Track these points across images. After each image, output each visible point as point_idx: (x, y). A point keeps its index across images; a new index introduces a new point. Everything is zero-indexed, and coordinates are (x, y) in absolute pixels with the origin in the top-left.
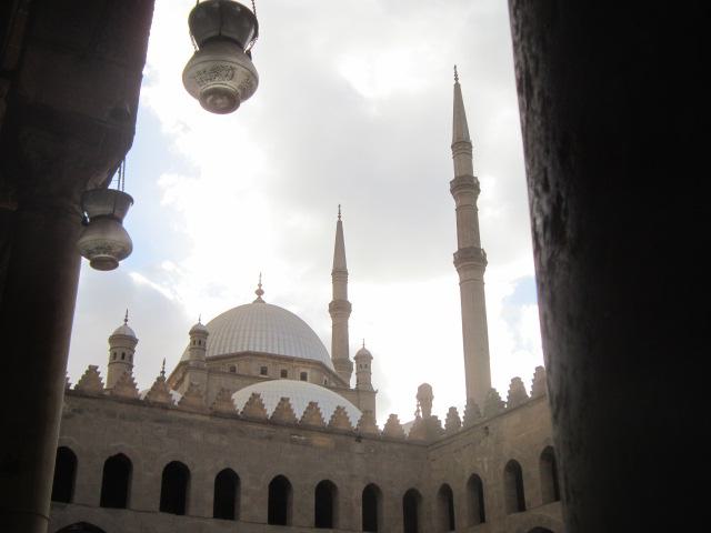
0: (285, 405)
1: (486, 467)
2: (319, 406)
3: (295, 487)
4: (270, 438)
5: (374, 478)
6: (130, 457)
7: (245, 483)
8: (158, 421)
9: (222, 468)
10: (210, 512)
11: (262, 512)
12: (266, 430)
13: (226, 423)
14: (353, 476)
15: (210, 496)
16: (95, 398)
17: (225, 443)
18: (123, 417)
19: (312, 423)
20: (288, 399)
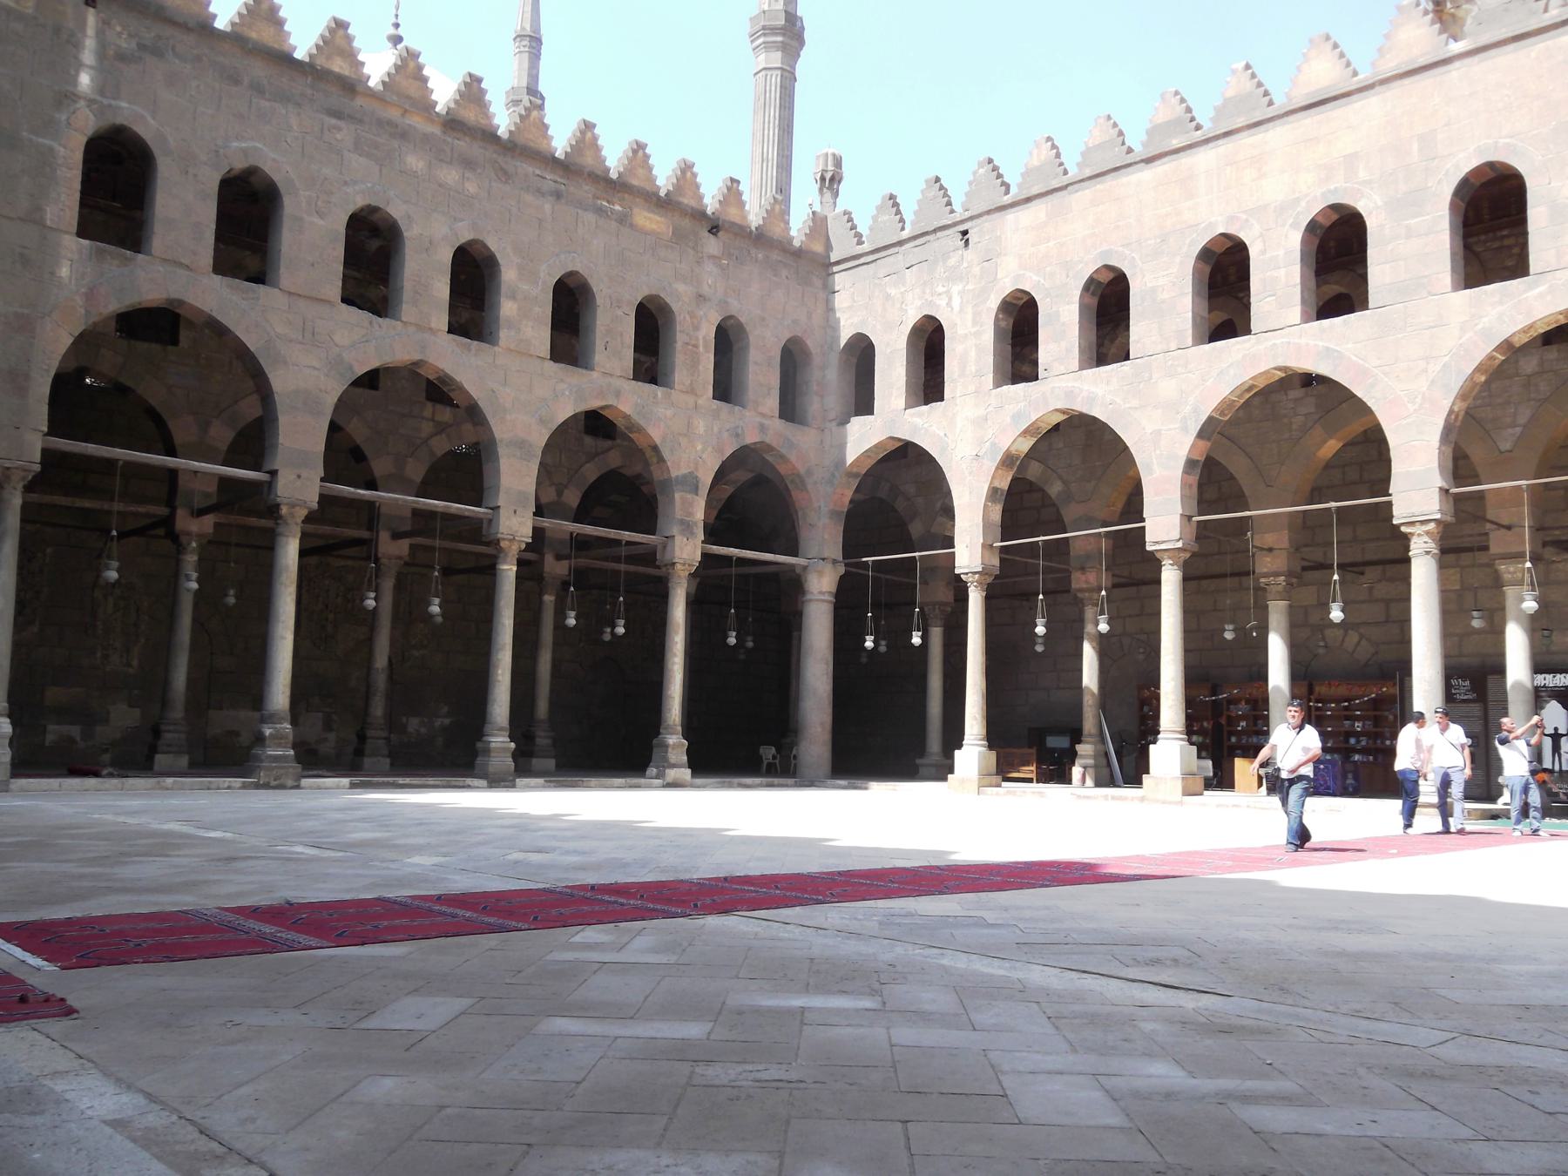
0: (589, 135)
1: (956, 302)
2: (648, 151)
3: (599, 301)
4: (558, 195)
5: (736, 307)
6: (276, 178)
7: (509, 274)
8: (338, 114)
9: (465, 236)
10: (440, 320)
11: (539, 335)
12: (551, 178)
13: (476, 150)
14: (701, 298)
15: (442, 289)
16: (184, 27)
17: (471, 188)
18: (257, 89)
19: (635, 182)
20: (594, 126)
